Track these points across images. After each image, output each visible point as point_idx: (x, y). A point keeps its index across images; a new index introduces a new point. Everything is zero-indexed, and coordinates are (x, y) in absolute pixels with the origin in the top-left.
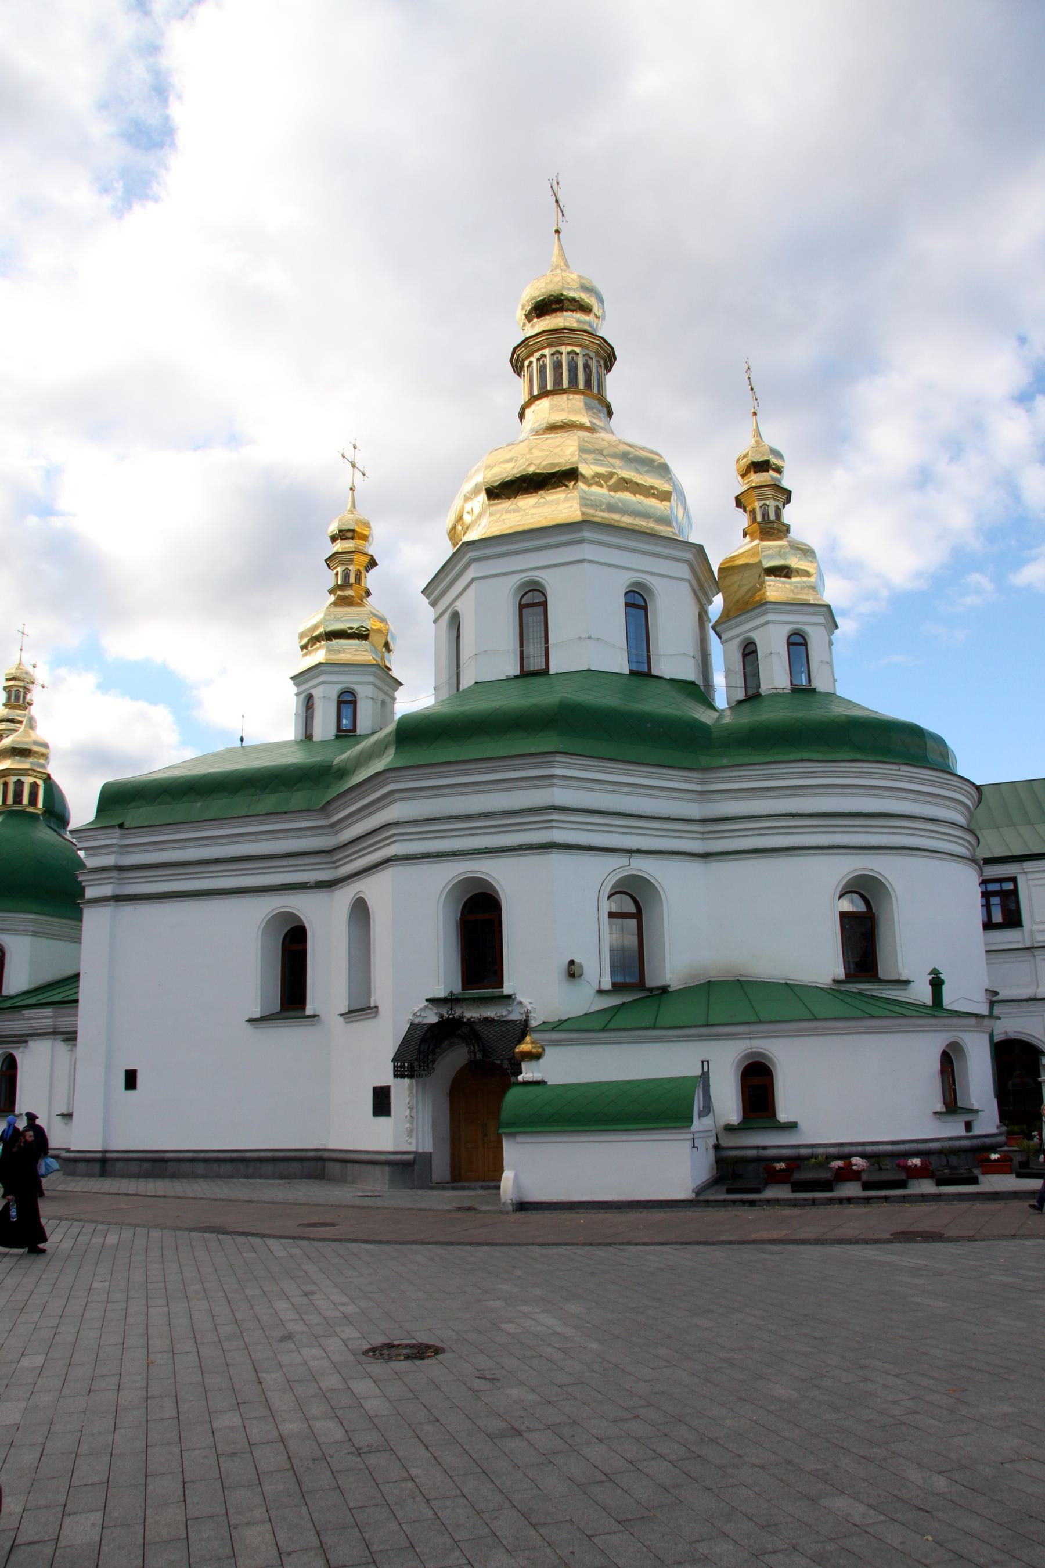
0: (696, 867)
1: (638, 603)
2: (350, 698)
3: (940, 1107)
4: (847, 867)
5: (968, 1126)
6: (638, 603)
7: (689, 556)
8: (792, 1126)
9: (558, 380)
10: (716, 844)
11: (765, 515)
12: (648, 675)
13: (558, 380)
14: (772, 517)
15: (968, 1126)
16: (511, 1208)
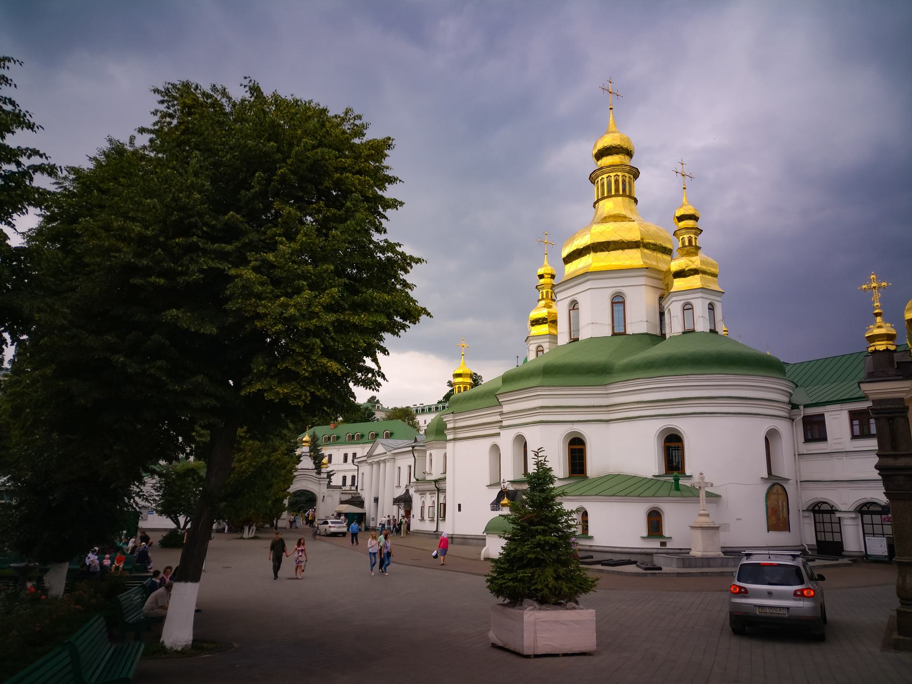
0: (603, 426)
1: (618, 301)
2: (540, 349)
3: (645, 534)
4: (659, 425)
5: (663, 544)
6: (618, 301)
7: (644, 273)
8: (591, 538)
9: (603, 193)
10: (607, 416)
11: (683, 243)
12: (624, 334)
13: (603, 193)
14: (687, 244)
15: (663, 544)
16: (482, 559)
